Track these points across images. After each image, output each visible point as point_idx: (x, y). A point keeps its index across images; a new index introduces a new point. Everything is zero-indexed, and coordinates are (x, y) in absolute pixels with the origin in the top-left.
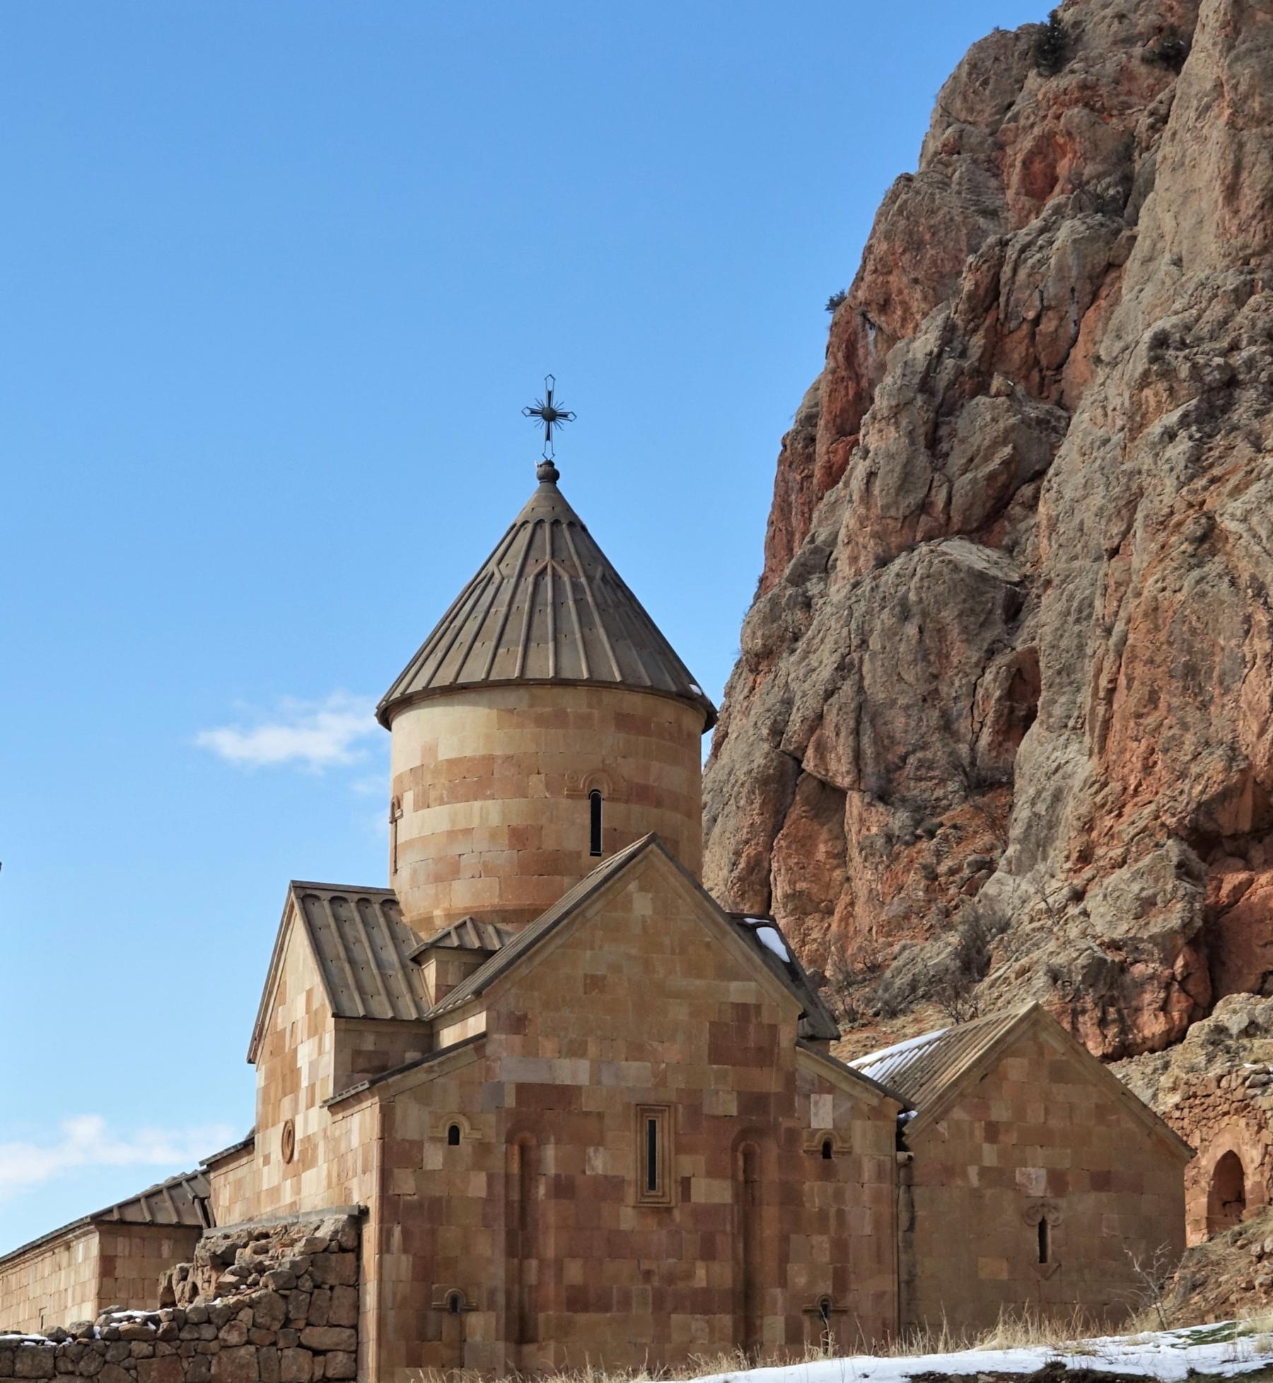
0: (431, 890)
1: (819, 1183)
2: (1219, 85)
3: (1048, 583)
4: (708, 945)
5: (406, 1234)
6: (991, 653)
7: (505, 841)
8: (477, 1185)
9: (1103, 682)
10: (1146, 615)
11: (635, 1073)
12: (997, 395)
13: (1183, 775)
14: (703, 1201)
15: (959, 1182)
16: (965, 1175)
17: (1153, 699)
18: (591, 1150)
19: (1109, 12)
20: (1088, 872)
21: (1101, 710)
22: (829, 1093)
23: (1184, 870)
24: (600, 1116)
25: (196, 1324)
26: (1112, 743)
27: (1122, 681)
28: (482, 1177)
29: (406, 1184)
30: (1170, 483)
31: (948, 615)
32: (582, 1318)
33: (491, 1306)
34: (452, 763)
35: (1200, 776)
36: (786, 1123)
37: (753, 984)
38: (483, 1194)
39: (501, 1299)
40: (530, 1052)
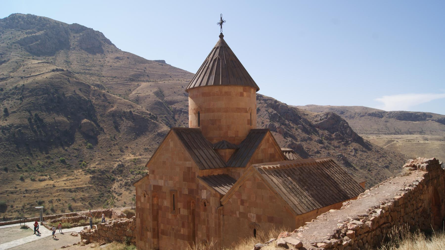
1: (204, 212)
4: (183, 153)
8: (148, 206)
14: (182, 214)
15: (234, 215)
18: (164, 200)
22: (205, 190)
24: (165, 193)
25: (124, 225)
28: (149, 204)
29: (139, 205)
33: (151, 232)
36: (197, 197)
37: (191, 162)
38: (149, 208)
40: (155, 178)
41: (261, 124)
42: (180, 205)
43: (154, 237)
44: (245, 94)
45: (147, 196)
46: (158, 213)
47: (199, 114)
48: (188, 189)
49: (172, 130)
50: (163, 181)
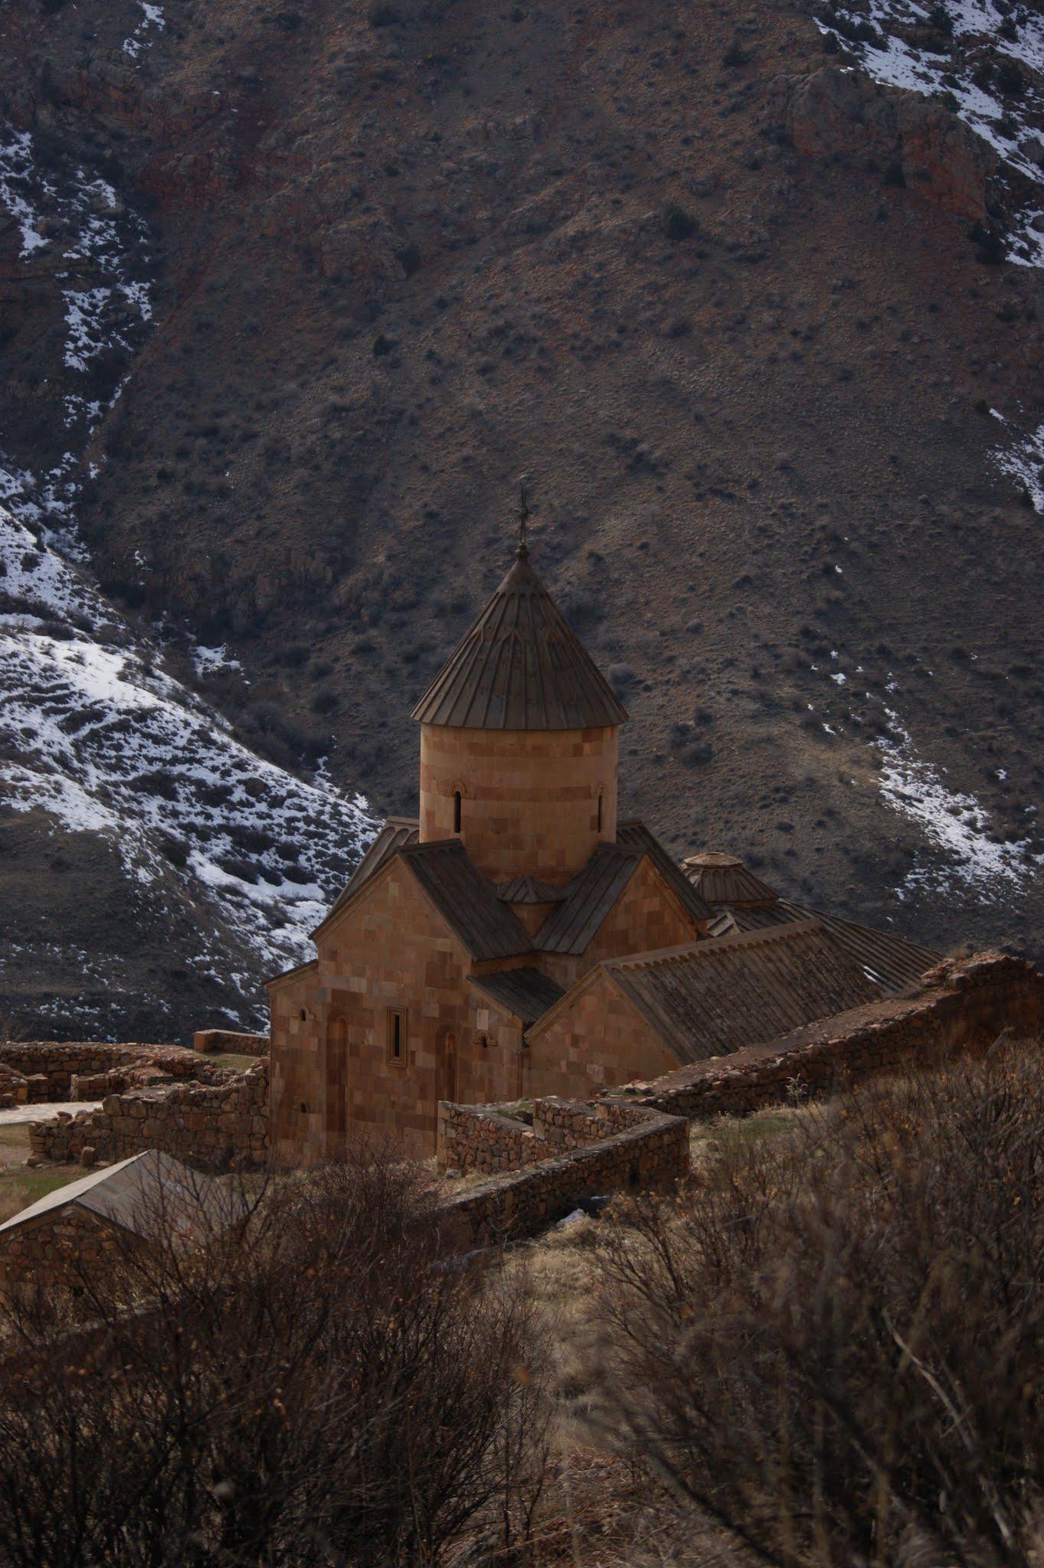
5: (281, 1067)
8: (313, 1045)
11: (389, 988)
16: (559, 1065)
24: (372, 1011)
28: (316, 1040)
32: (362, 1123)
37: (448, 941)
38: (316, 1049)
39: (325, 1108)
40: (338, 972)
41: (712, 72)
42: (414, 1044)
43: (329, 1126)
44: (587, 747)
45: (308, 1016)
46: (343, 1064)
47: (458, 797)
48: (440, 1006)
49: (397, 855)
50: (364, 981)
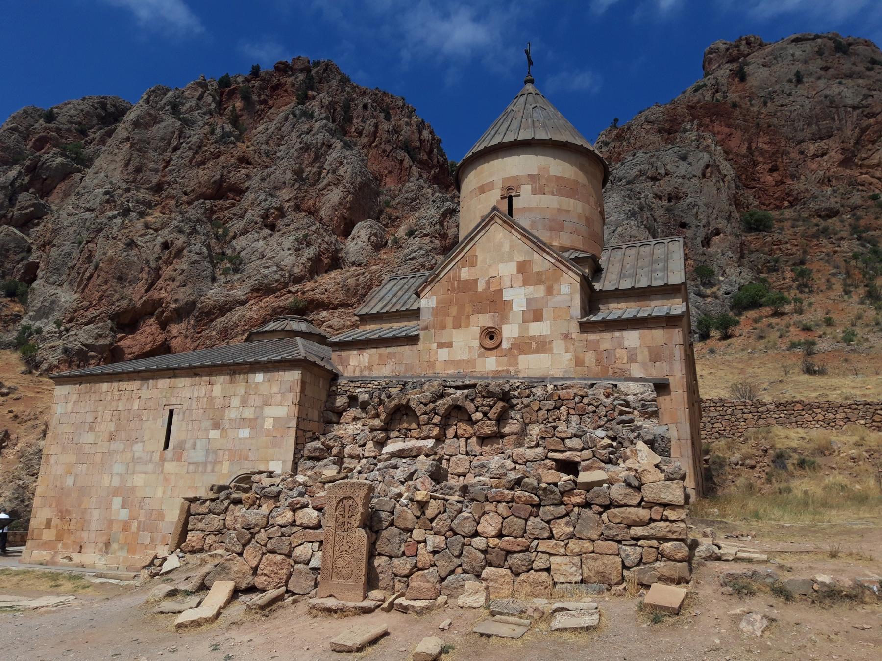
0: (548, 233)
2: (128, 139)
3: (54, 245)
6: (22, 260)
7: (583, 222)
9: (87, 274)
10: (108, 260)
12: (32, 193)
13: (113, 304)
17: (106, 282)
19: (68, 114)
20: (72, 324)
21: (85, 282)
23: (111, 329)
26: (86, 290)
27: (95, 275)
30: (115, 229)
31: (12, 245)
34: (558, 178)
35: (118, 306)
